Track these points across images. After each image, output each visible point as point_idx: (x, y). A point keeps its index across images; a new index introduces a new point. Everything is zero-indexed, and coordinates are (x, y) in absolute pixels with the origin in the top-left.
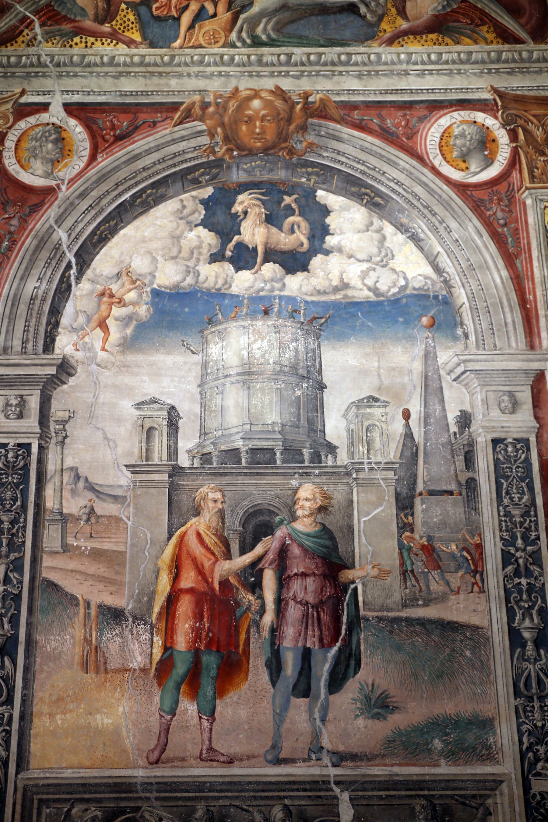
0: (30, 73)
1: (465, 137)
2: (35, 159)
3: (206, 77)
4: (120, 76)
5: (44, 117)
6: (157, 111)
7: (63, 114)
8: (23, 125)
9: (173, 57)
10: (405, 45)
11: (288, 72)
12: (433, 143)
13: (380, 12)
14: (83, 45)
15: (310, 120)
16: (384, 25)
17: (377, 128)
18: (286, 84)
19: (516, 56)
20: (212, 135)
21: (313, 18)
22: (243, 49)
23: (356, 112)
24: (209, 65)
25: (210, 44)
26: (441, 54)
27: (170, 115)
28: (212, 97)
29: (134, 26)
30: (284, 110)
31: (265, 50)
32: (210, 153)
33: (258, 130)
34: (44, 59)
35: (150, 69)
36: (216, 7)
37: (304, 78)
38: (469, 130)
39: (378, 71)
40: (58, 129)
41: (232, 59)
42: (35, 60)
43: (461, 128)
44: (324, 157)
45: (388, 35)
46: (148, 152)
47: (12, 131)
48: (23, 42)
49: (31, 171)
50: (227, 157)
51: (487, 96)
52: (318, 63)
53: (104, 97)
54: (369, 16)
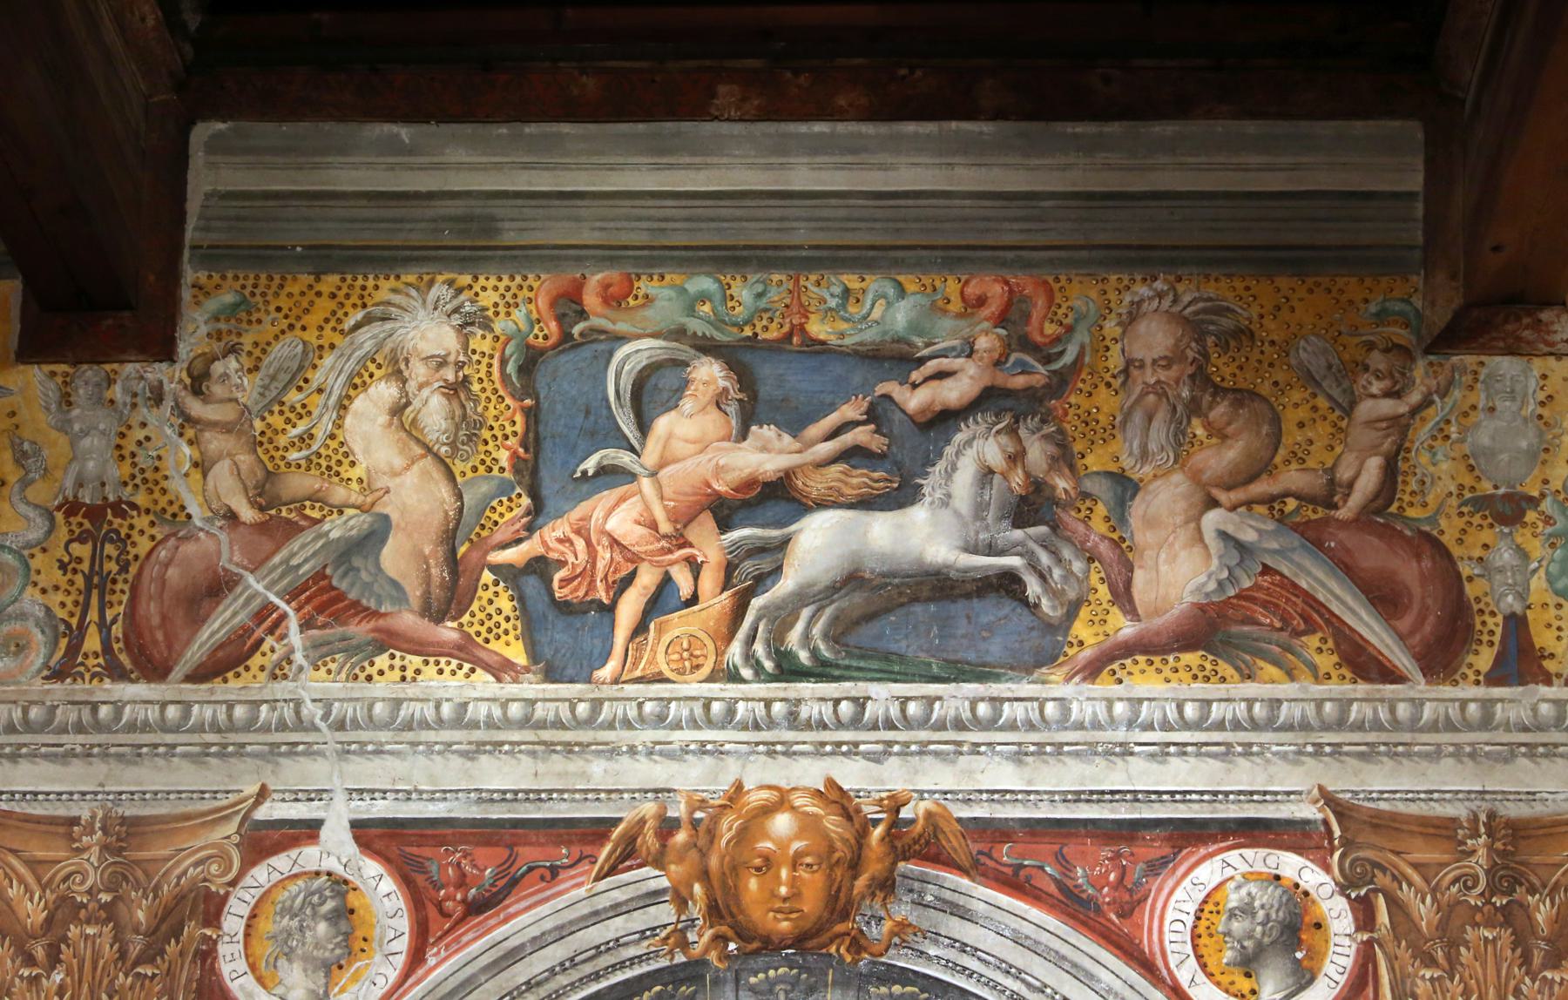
0: (279, 745)
1: (1254, 915)
2: (290, 960)
4: (477, 752)
5: (309, 856)
6: (559, 842)
7: (351, 848)
8: (261, 875)
9: (597, 704)
10: (1126, 680)
11: (856, 744)
13: (1072, 594)
14: (397, 674)
15: (902, 866)
16: (1080, 629)
18: (852, 775)
19: (1383, 715)
20: (681, 902)
21: (918, 608)
22: (755, 686)
24: (677, 726)
25: (681, 672)
26: (1209, 702)
27: (588, 850)
28: (682, 806)
29: (509, 626)
30: (845, 841)
31: (806, 688)
32: (677, 945)
33: (783, 890)
34: (311, 711)
35: (546, 735)
36: (696, 578)
37: (893, 759)
38: (1265, 897)
39: (1062, 745)
40: (340, 886)
41: (731, 712)
42: (288, 713)
43: (1244, 891)
44: (929, 958)
45: (1087, 653)
46: (539, 943)
47: (239, 892)
48: (262, 668)
49: (280, 990)
50: (713, 956)
52: (924, 723)
53: (442, 805)
54: (1045, 604)
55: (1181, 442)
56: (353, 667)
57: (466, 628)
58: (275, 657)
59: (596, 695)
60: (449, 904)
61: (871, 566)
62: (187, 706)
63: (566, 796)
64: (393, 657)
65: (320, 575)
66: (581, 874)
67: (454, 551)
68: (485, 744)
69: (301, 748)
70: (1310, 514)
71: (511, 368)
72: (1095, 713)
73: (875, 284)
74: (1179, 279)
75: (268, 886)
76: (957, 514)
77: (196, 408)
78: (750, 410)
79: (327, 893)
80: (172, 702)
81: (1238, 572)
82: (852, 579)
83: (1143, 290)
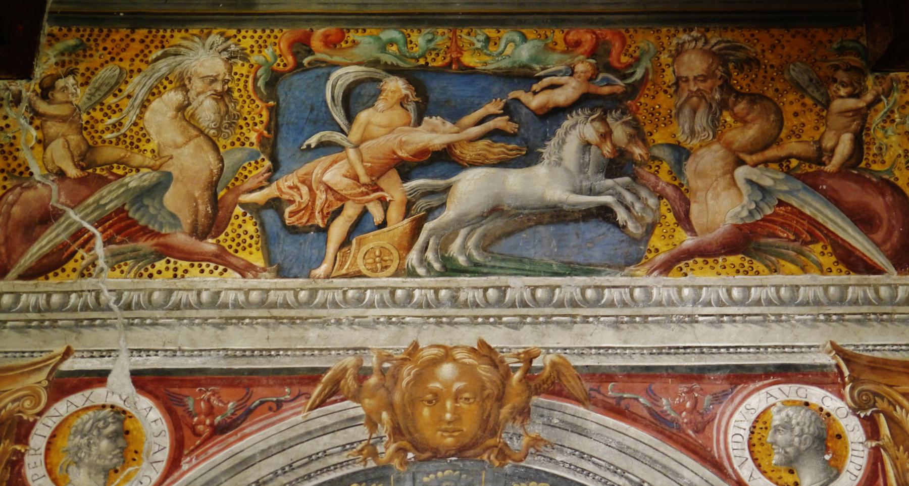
0: (82, 320)
1: (792, 430)
2: (78, 467)
3: (366, 326)
4: (226, 324)
5: (98, 395)
6: (283, 384)
7: (130, 389)
8: (62, 408)
9: (313, 292)
10: (690, 274)
11: (500, 317)
12: (739, 438)
13: (649, 219)
14: (171, 273)
15: (535, 399)
16: (655, 241)
17: (645, 413)
18: (496, 338)
20: (373, 425)
21: (541, 229)
22: (427, 279)
23: (610, 385)
24: (371, 305)
25: (375, 271)
26: (749, 288)
27: (304, 389)
28: (374, 359)
29: (253, 242)
30: (492, 382)
31: (463, 281)
32: (369, 455)
33: (448, 416)
34: (108, 297)
35: (276, 312)
37: (526, 327)
38: (799, 417)
39: (647, 316)
40: (120, 414)
41: (410, 296)
42: (90, 299)
43: (783, 414)
44: (557, 463)
45: (661, 257)
46: (267, 454)
47: (44, 419)
48: (74, 270)
50: (396, 463)
51: (826, 359)
52: (548, 302)
53: (198, 360)
54: (631, 226)
55: (716, 124)
56: (139, 269)
57: (221, 243)
58: (84, 262)
59: (313, 286)
60: (200, 428)
61: (508, 203)
62: (17, 295)
63: (289, 353)
64: (168, 262)
65: (120, 210)
66: (299, 406)
67: (215, 194)
68: (231, 318)
69: (98, 322)
70: (806, 168)
71: (260, 83)
72: (669, 295)
73: (507, 34)
74: (708, 30)
75: (66, 415)
76: (567, 170)
77: (43, 107)
78: (423, 108)
79: (110, 420)
80: (7, 293)
81: (762, 205)
82: (495, 211)
83: (685, 37)
